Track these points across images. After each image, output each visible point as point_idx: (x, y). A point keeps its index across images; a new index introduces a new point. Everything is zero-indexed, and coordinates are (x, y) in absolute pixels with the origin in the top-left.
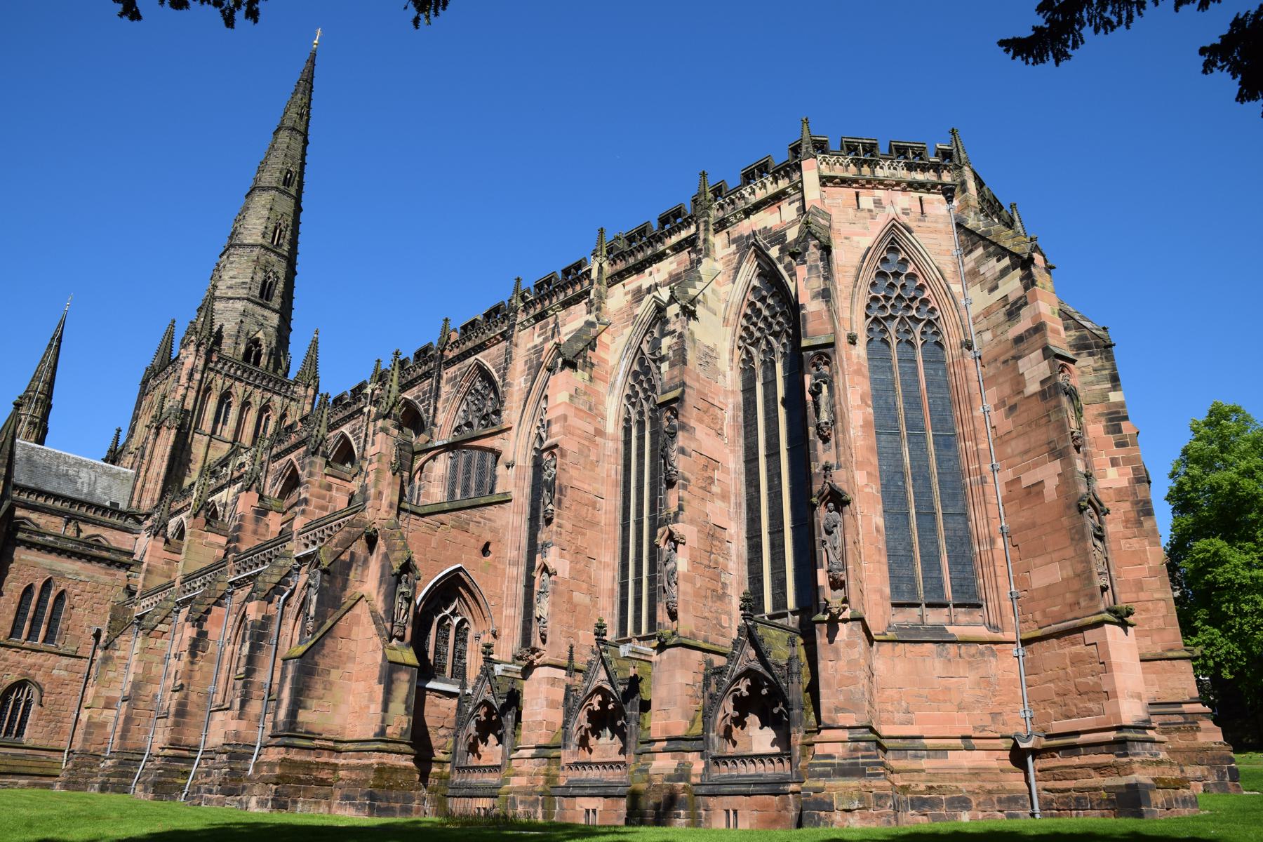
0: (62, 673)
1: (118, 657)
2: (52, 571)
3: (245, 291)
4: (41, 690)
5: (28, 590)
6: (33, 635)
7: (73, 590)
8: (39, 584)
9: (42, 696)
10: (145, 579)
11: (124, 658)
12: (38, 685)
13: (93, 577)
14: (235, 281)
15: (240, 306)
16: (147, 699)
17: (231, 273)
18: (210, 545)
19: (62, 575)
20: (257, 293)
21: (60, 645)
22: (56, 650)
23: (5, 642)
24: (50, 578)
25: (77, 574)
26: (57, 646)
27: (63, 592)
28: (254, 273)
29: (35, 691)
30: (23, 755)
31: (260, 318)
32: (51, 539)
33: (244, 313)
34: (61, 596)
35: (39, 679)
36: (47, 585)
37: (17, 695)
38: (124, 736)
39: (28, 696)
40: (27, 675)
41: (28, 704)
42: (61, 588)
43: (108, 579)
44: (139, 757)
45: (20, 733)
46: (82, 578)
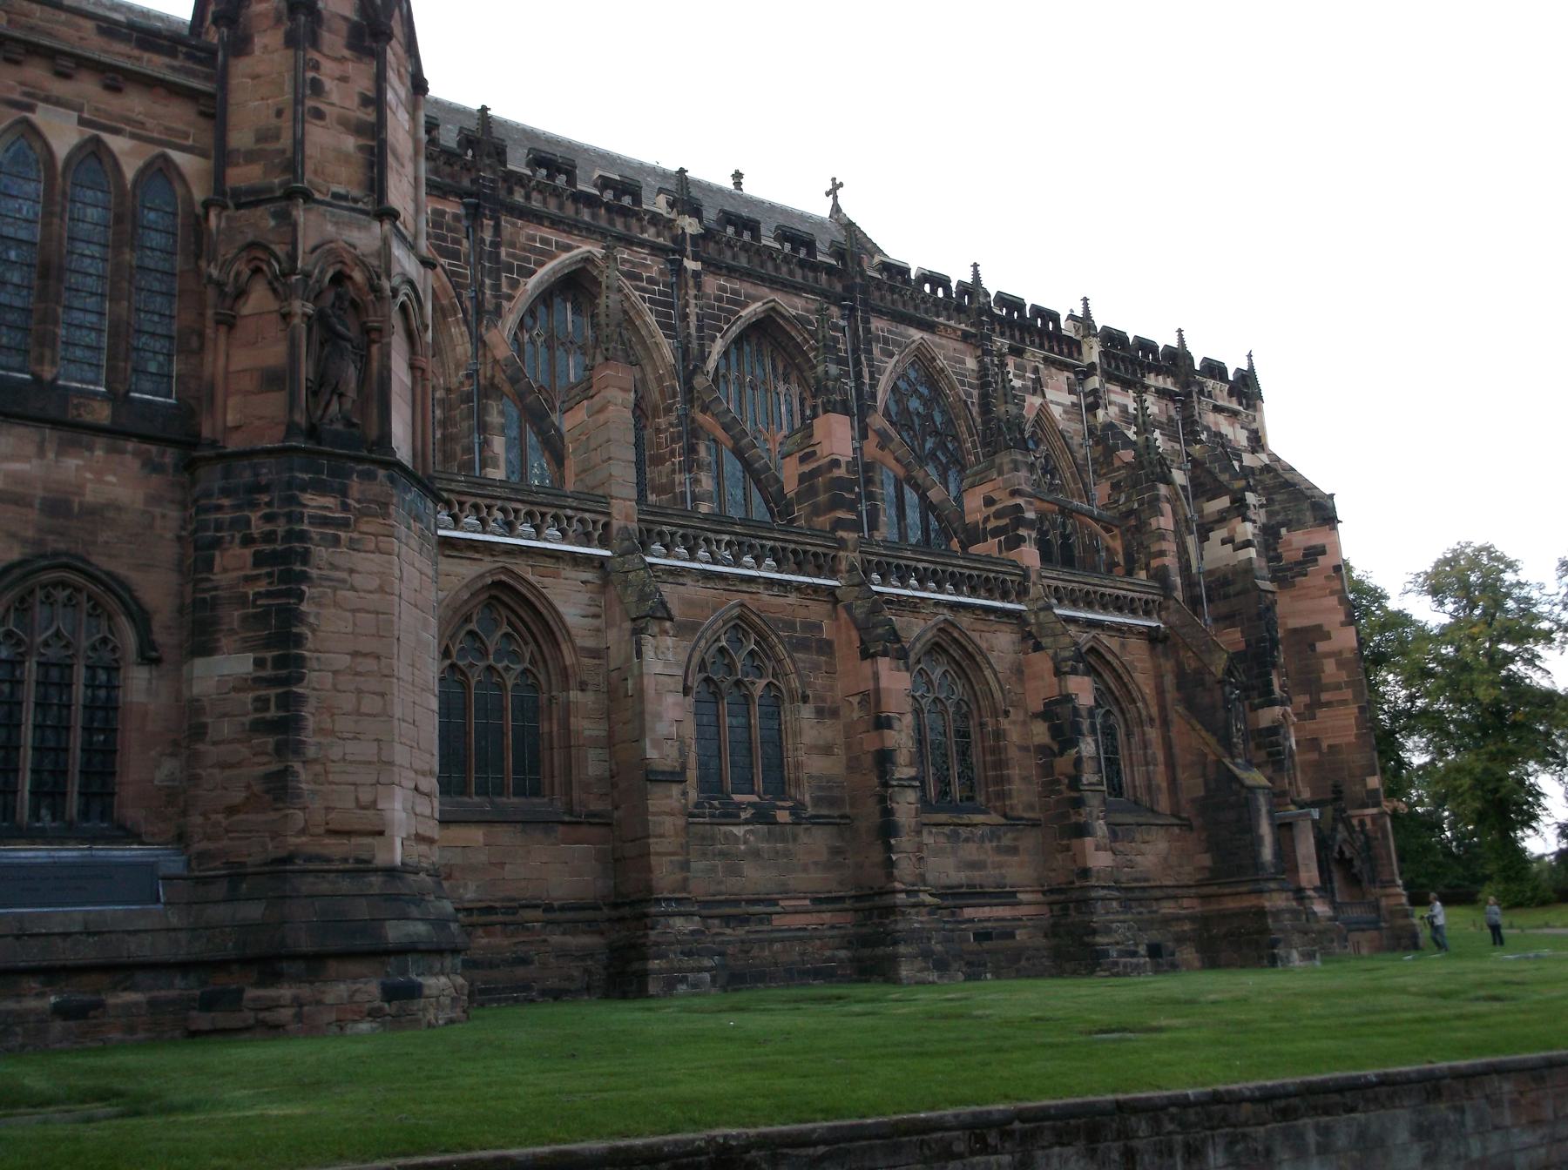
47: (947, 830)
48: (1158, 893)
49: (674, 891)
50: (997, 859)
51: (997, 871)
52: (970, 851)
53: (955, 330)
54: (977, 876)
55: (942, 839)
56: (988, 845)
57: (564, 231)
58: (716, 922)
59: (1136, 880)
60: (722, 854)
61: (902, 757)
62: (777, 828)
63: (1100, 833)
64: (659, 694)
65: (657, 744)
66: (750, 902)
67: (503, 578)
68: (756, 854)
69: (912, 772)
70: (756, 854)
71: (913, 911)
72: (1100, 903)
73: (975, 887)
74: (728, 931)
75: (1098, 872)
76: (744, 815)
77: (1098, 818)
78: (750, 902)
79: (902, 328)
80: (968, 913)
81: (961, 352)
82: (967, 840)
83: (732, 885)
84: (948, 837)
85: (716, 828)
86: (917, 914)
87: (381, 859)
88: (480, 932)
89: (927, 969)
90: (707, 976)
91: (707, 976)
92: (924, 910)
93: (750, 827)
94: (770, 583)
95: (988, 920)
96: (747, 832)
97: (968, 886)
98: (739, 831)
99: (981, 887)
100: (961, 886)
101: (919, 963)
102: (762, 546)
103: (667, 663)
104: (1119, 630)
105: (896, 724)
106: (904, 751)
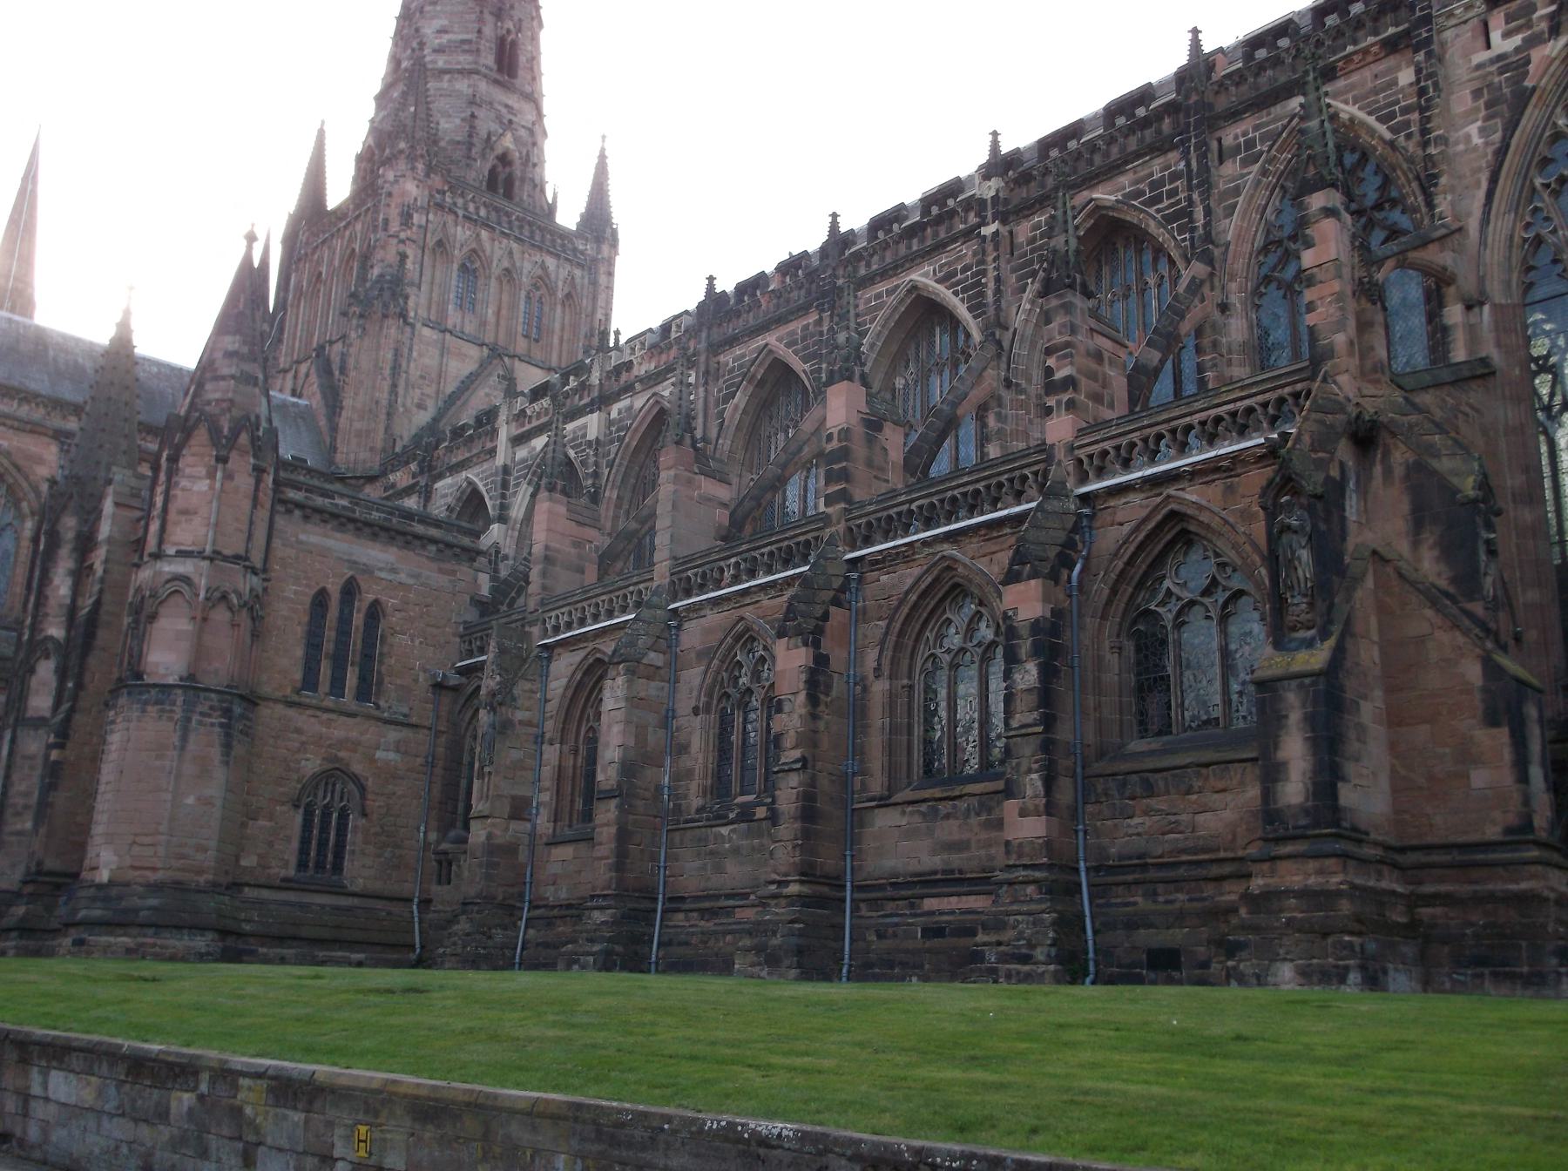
0: (392, 756)
1: (521, 722)
2: (353, 563)
3: (470, 58)
4: (363, 789)
5: (320, 600)
6: (337, 687)
7: (391, 602)
8: (334, 589)
9: (363, 797)
10: (544, 574)
11: (529, 724)
12: (355, 779)
13: (417, 576)
14: (445, 38)
15: (463, 85)
16: (648, 795)
17: (438, 23)
18: (707, 500)
19: (368, 570)
20: (489, 59)
21: (382, 703)
22: (377, 713)
23: (296, 698)
24: (352, 577)
25: (393, 570)
26: (378, 707)
27: (376, 604)
28: (481, 20)
29: (351, 786)
30: (349, 909)
31: (504, 110)
32: (344, 502)
33: (472, 101)
34: (375, 612)
35: (357, 768)
36: (350, 590)
37: (325, 797)
38: (620, 866)
39: (342, 799)
40: (337, 759)
41: (343, 816)
42: (371, 597)
43: (443, 581)
44: (646, 905)
45: (338, 867)
46: (403, 577)
47: (923, 807)
48: (1215, 870)
49: (603, 889)
50: (984, 836)
51: (983, 852)
52: (950, 830)
53: (1366, 51)
54: (956, 860)
55: (917, 819)
56: (974, 821)
57: (891, 277)
58: (695, 914)
59: (1183, 851)
60: (712, 853)
61: (788, 741)
62: (755, 824)
63: (1029, 792)
64: (609, 726)
65: (604, 770)
66: (729, 896)
67: (598, 655)
68: (736, 851)
69: (797, 754)
70: (736, 851)
71: (773, 902)
72: (1005, 888)
73: (952, 872)
74: (702, 923)
75: (1020, 845)
76: (732, 816)
77: (1030, 771)
78: (729, 896)
79: (1277, 110)
80: (930, 904)
81: (1389, 71)
82: (947, 816)
83: (716, 882)
84: (924, 815)
85: (709, 830)
86: (776, 905)
87: (97, 881)
88: (558, 922)
89: (759, 964)
90: (591, 959)
91: (591, 959)
92: (783, 902)
93: (731, 827)
94: (763, 588)
95: (952, 912)
96: (731, 831)
97: (944, 872)
98: (725, 831)
99: (961, 872)
100: (935, 873)
101: (751, 957)
102: (762, 555)
103: (616, 699)
104: (1218, 469)
105: (787, 708)
106: (792, 733)
